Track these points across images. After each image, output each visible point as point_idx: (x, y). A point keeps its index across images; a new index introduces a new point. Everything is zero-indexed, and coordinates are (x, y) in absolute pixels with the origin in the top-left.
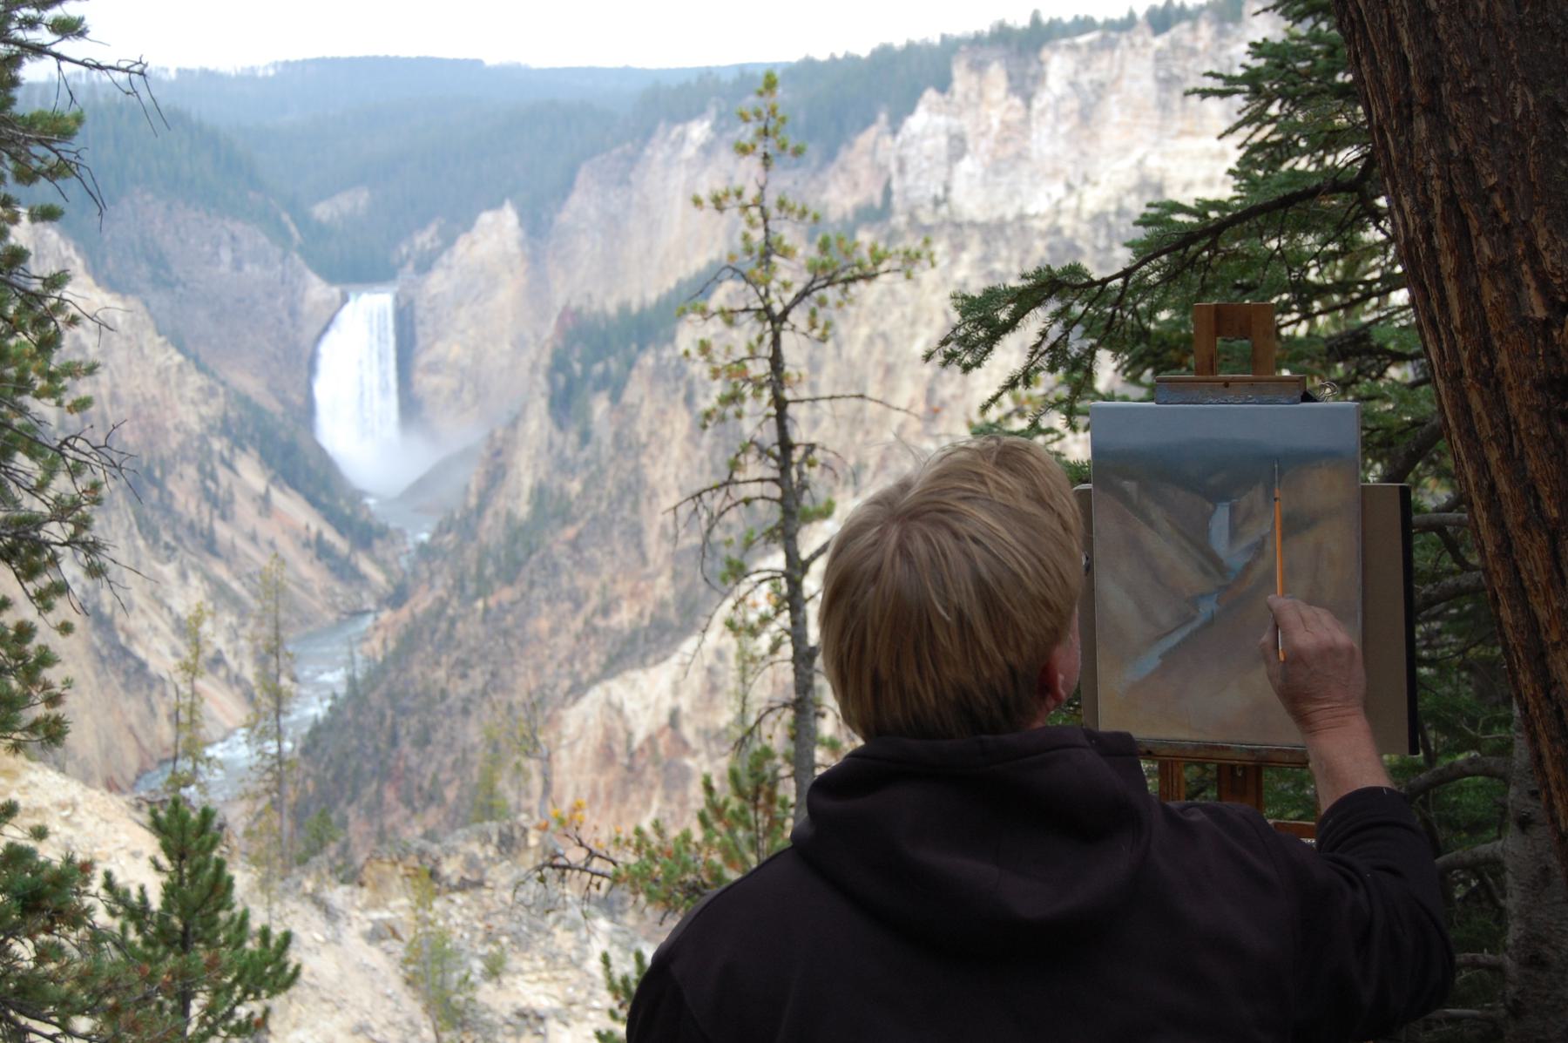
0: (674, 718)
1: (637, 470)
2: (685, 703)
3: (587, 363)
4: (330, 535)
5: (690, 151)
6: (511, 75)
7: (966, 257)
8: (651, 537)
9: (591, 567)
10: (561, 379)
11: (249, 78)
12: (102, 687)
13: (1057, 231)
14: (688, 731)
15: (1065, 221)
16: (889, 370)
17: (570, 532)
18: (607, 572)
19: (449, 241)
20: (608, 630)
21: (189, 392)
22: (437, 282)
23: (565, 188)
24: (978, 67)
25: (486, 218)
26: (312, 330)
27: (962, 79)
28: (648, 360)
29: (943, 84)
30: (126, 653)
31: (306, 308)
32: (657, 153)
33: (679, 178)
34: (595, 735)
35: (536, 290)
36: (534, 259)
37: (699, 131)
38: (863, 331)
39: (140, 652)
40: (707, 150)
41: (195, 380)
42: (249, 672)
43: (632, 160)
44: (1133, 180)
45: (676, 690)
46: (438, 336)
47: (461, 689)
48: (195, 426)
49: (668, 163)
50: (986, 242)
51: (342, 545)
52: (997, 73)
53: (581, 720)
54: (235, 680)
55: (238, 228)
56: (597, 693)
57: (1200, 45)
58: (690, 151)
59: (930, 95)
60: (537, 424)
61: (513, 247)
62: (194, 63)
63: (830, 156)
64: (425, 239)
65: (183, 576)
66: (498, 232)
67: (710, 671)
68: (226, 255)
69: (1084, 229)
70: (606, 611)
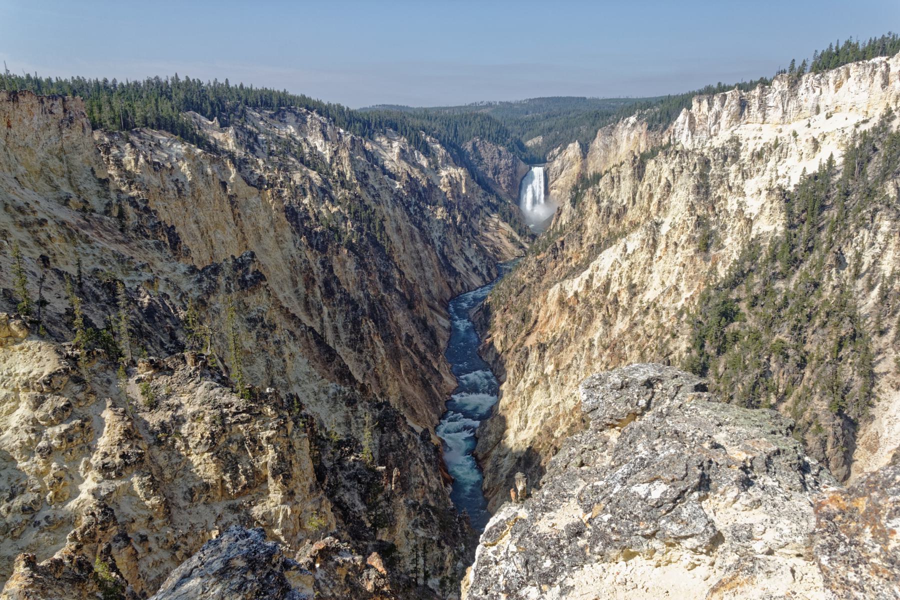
0: (576, 294)
1: (582, 221)
2: (580, 290)
3: (583, 189)
4: (515, 235)
5: (629, 125)
6: (594, 101)
7: (675, 162)
8: (585, 240)
9: (568, 249)
10: (574, 194)
11: (520, 104)
12: (441, 275)
13: (702, 155)
14: (580, 299)
15: (705, 151)
16: (651, 196)
17: (562, 239)
18: (571, 250)
19: (560, 152)
20: (567, 267)
21: (480, 195)
22: (557, 164)
23: (595, 137)
24: (700, 102)
25: (571, 145)
26: (520, 176)
27: (695, 104)
28: (591, 189)
29: (689, 107)
30: (450, 266)
31: (519, 171)
32: (620, 126)
33: (625, 133)
34: (557, 296)
35: (584, 166)
36: (584, 157)
37: (632, 119)
38: (646, 183)
39: (454, 265)
40: (634, 125)
41: (481, 191)
42: (485, 272)
43: (613, 128)
44: (728, 137)
45: (579, 286)
46: (556, 179)
47: (527, 281)
48: (480, 203)
49: (623, 129)
50: (680, 157)
51: (518, 238)
52: (705, 103)
53: (554, 292)
54: (480, 274)
55: (501, 148)
56: (558, 285)
57: (756, 95)
58: (629, 125)
59: (684, 110)
60: (568, 206)
61: (578, 154)
62: (504, 100)
63: (665, 128)
64: (556, 151)
65: (470, 245)
66: (573, 149)
67: (587, 281)
68: (497, 156)
69: (711, 153)
70: (567, 261)
